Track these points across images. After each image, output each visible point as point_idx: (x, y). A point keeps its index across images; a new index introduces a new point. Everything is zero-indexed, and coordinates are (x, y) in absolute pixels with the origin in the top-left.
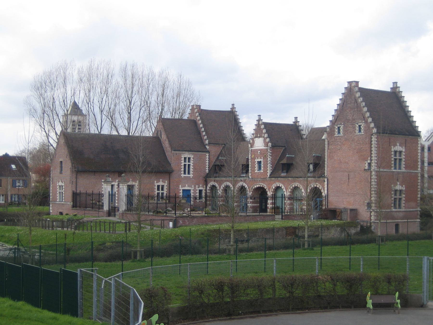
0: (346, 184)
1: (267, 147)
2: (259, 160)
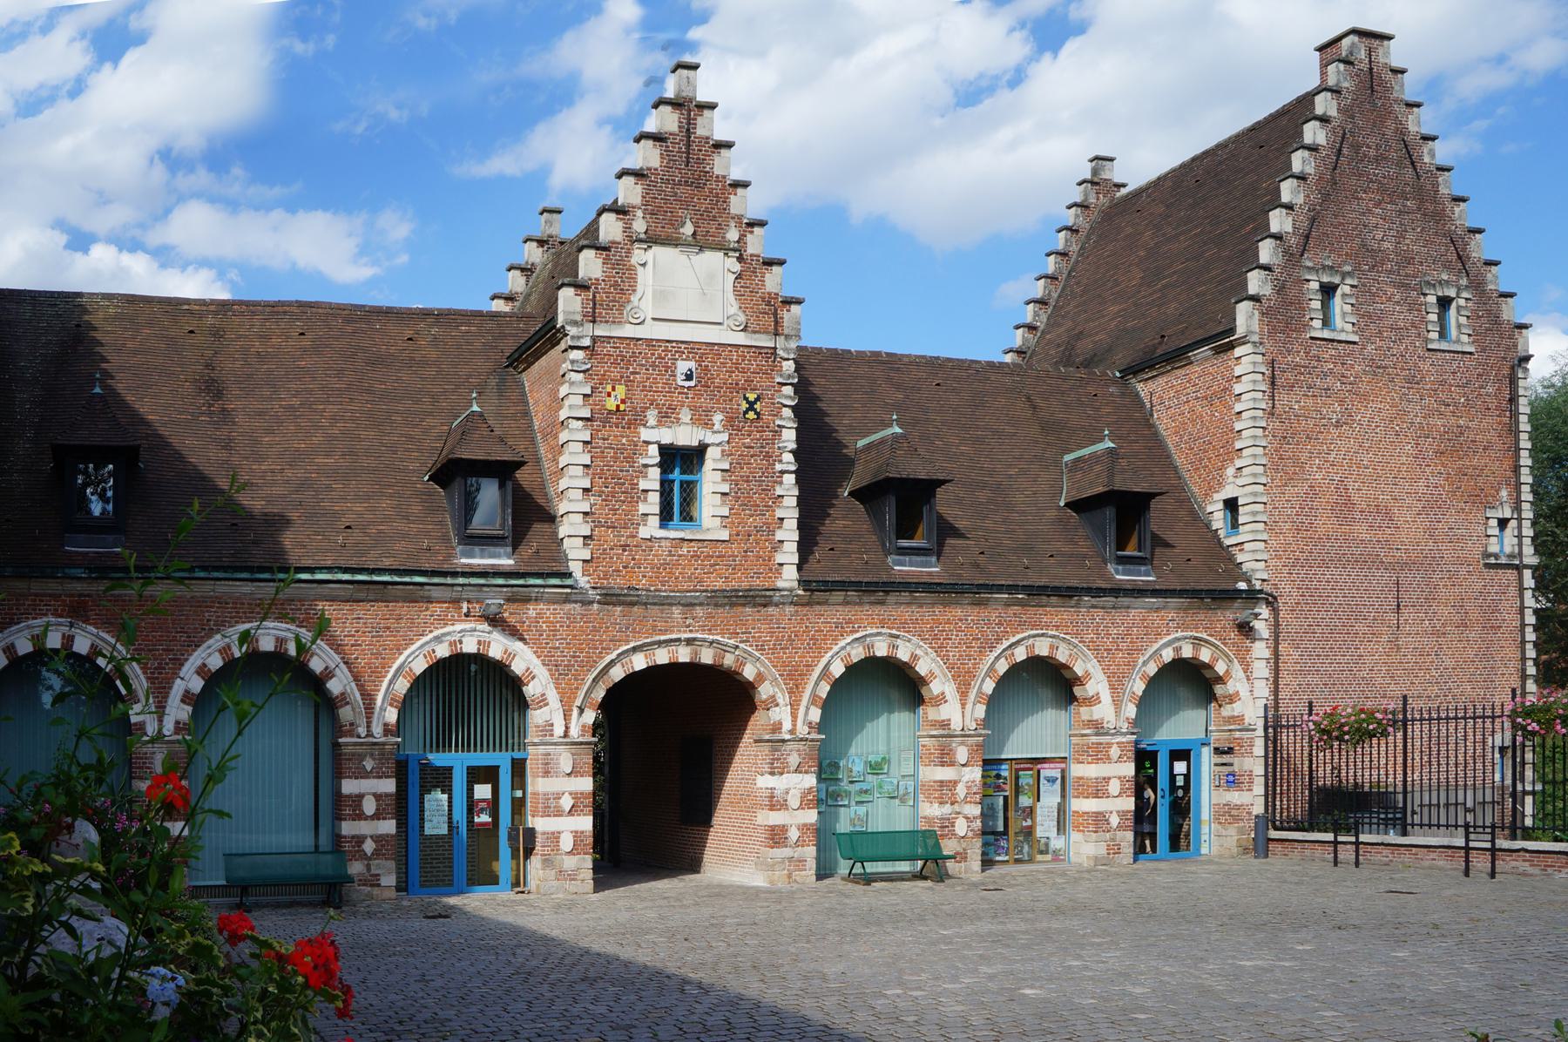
0: (1385, 638)
1: (776, 334)
2: (684, 435)
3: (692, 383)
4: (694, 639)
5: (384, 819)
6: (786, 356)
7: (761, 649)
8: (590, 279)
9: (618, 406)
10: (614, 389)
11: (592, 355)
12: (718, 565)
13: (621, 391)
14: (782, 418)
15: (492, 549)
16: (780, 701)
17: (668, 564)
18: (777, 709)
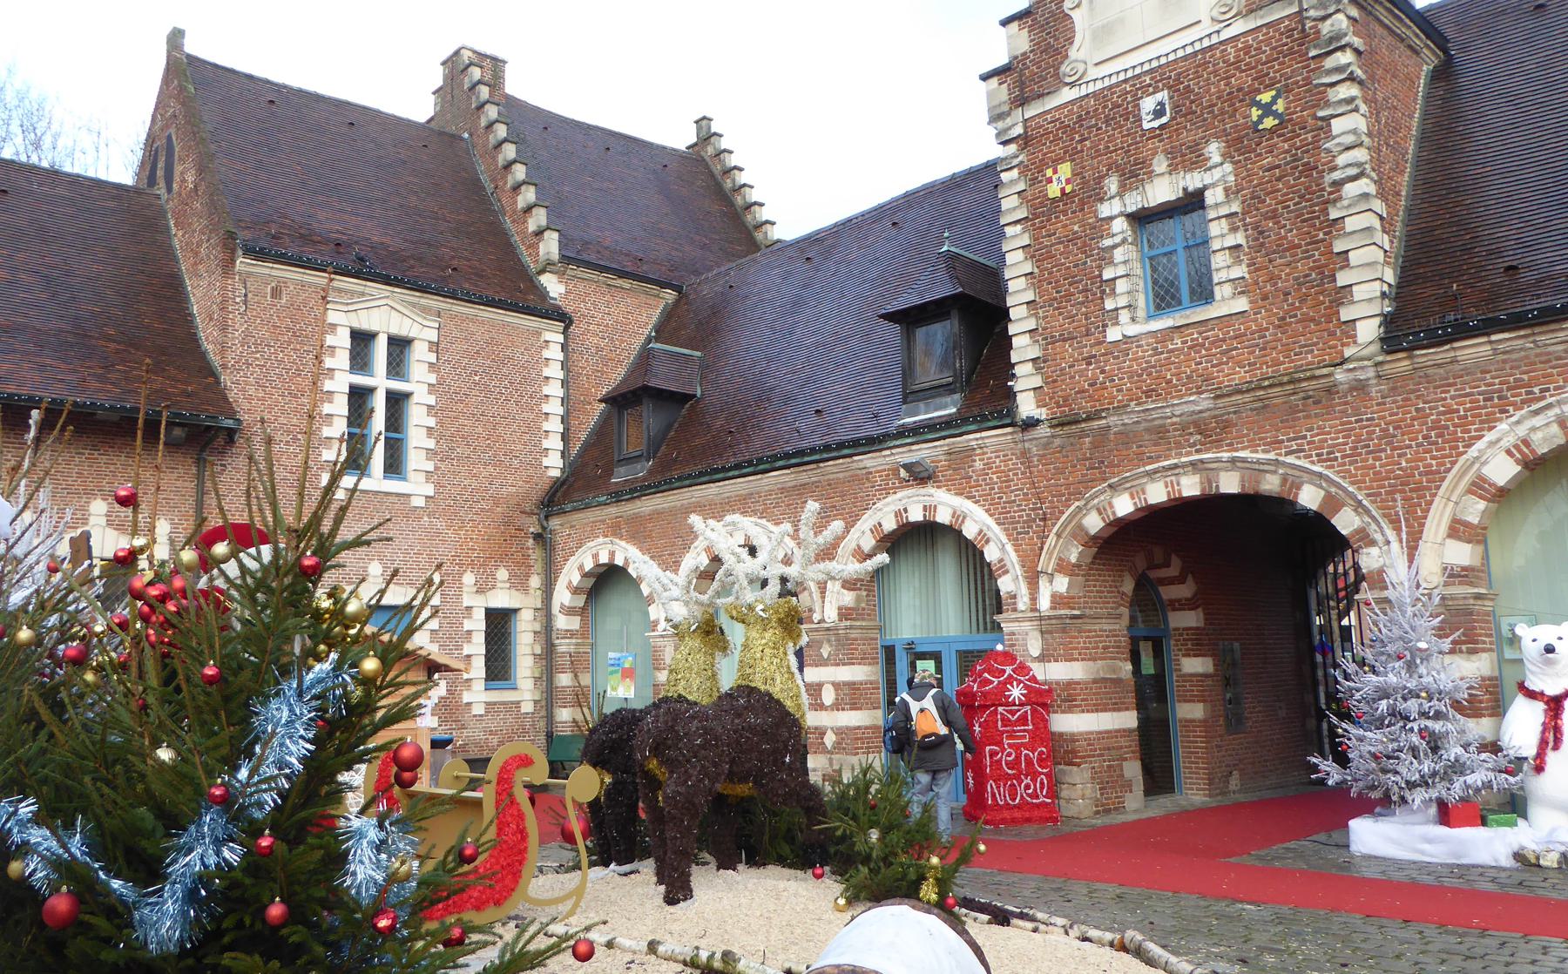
3: (1164, 120)
4: (1202, 461)
5: (843, 709)
6: (1321, 13)
7: (1328, 460)
8: (1016, 58)
9: (1063, 190)
10: (1055, 172)
11: (1026, 143)
12: (1236, 348)
13: (1065, 170)
14: (1328, 104)
15: (938, 400)
16: (1378, 537)
17: (1154, 367)
18: (1374, 551)
